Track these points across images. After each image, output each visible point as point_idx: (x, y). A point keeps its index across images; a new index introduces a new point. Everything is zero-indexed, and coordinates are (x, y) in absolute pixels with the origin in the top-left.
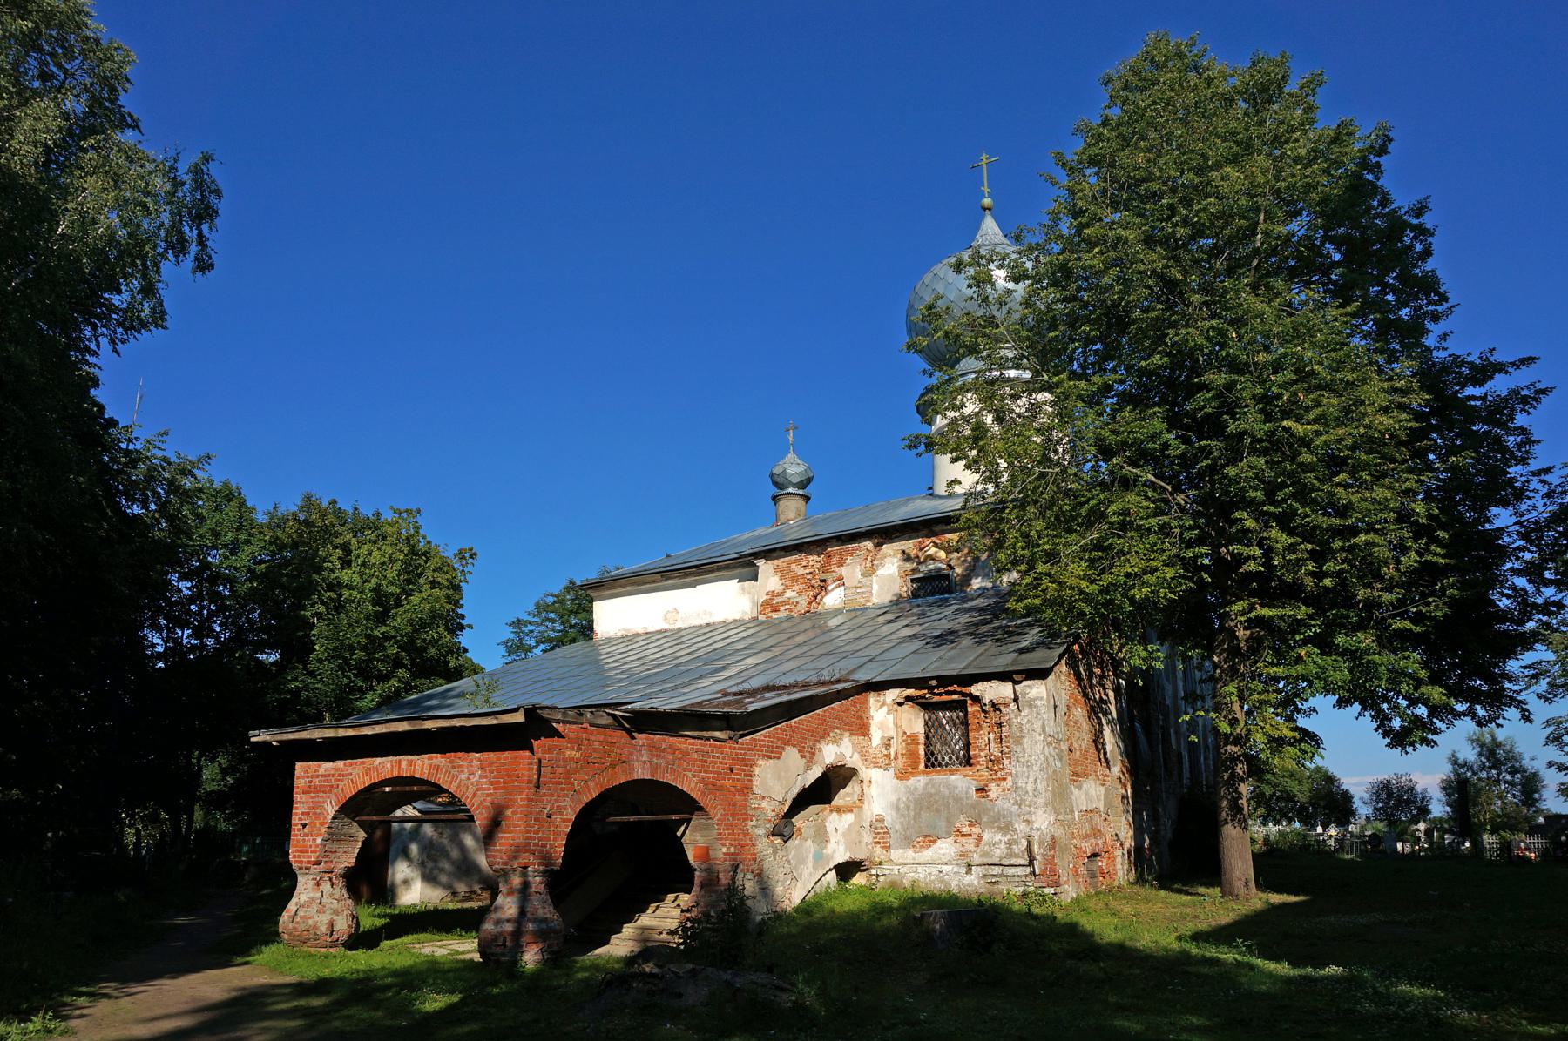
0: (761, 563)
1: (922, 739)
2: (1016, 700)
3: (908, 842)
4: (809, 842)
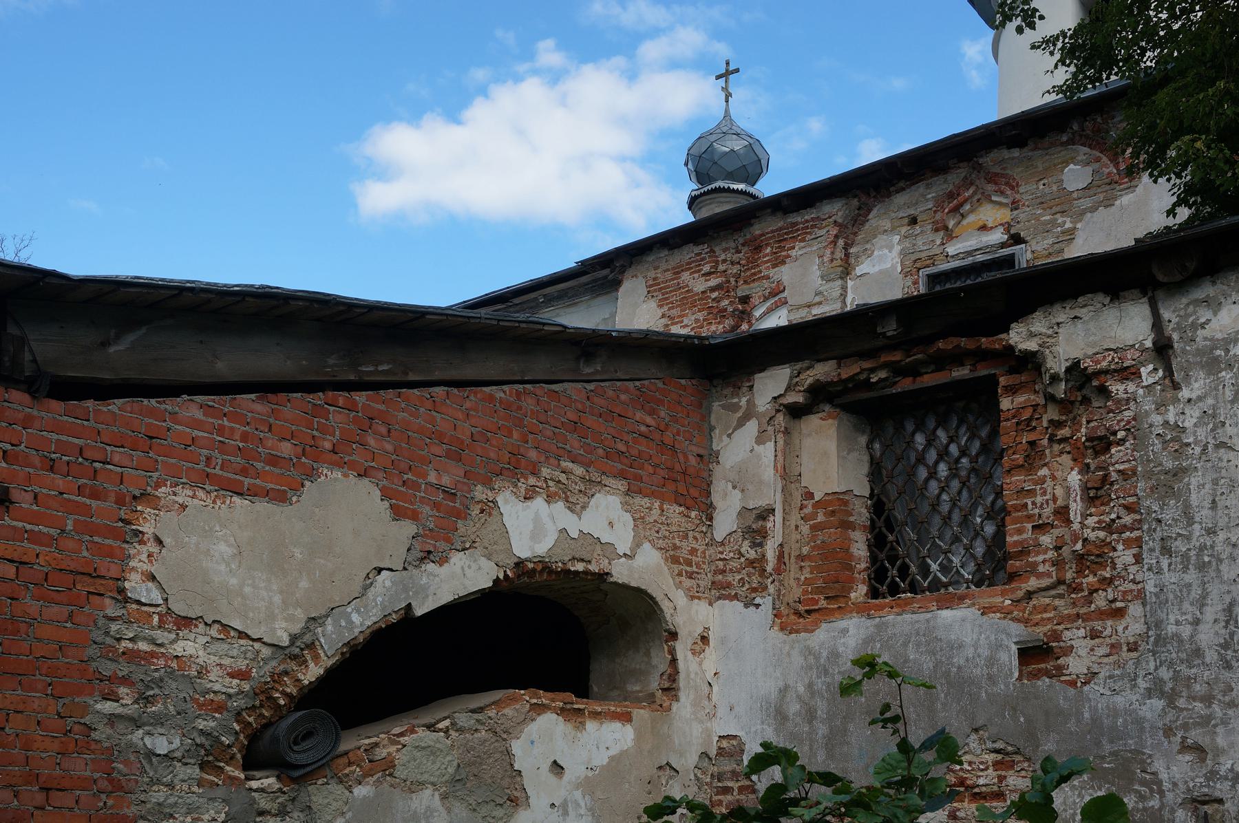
1: (861, 513)
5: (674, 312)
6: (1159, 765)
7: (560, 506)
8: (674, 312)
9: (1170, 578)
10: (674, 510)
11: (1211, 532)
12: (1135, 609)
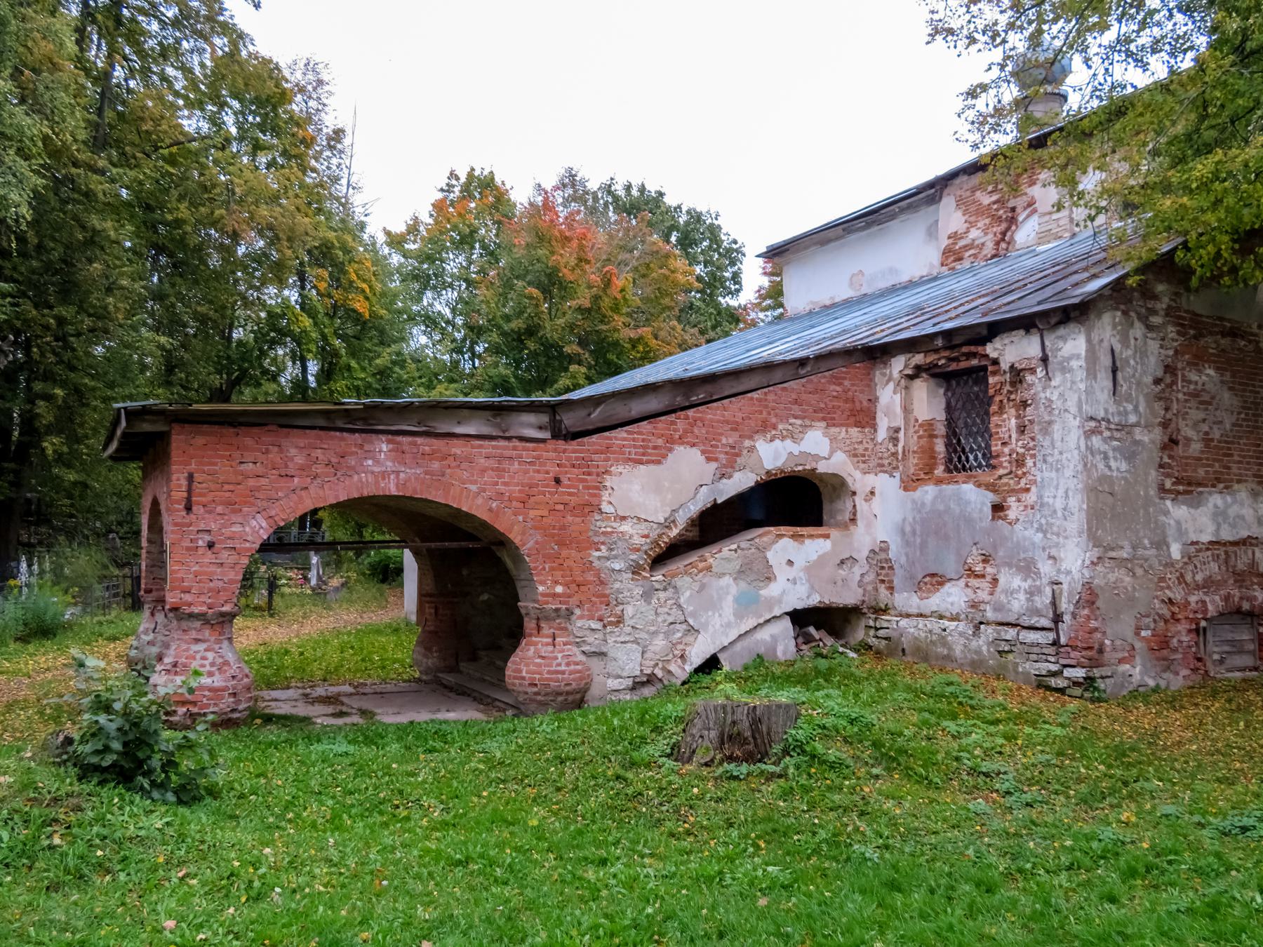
1: (941, 429)
4: (727, 580)
7: (788, 442)
10: (854, 431)
11: (1061, 453)
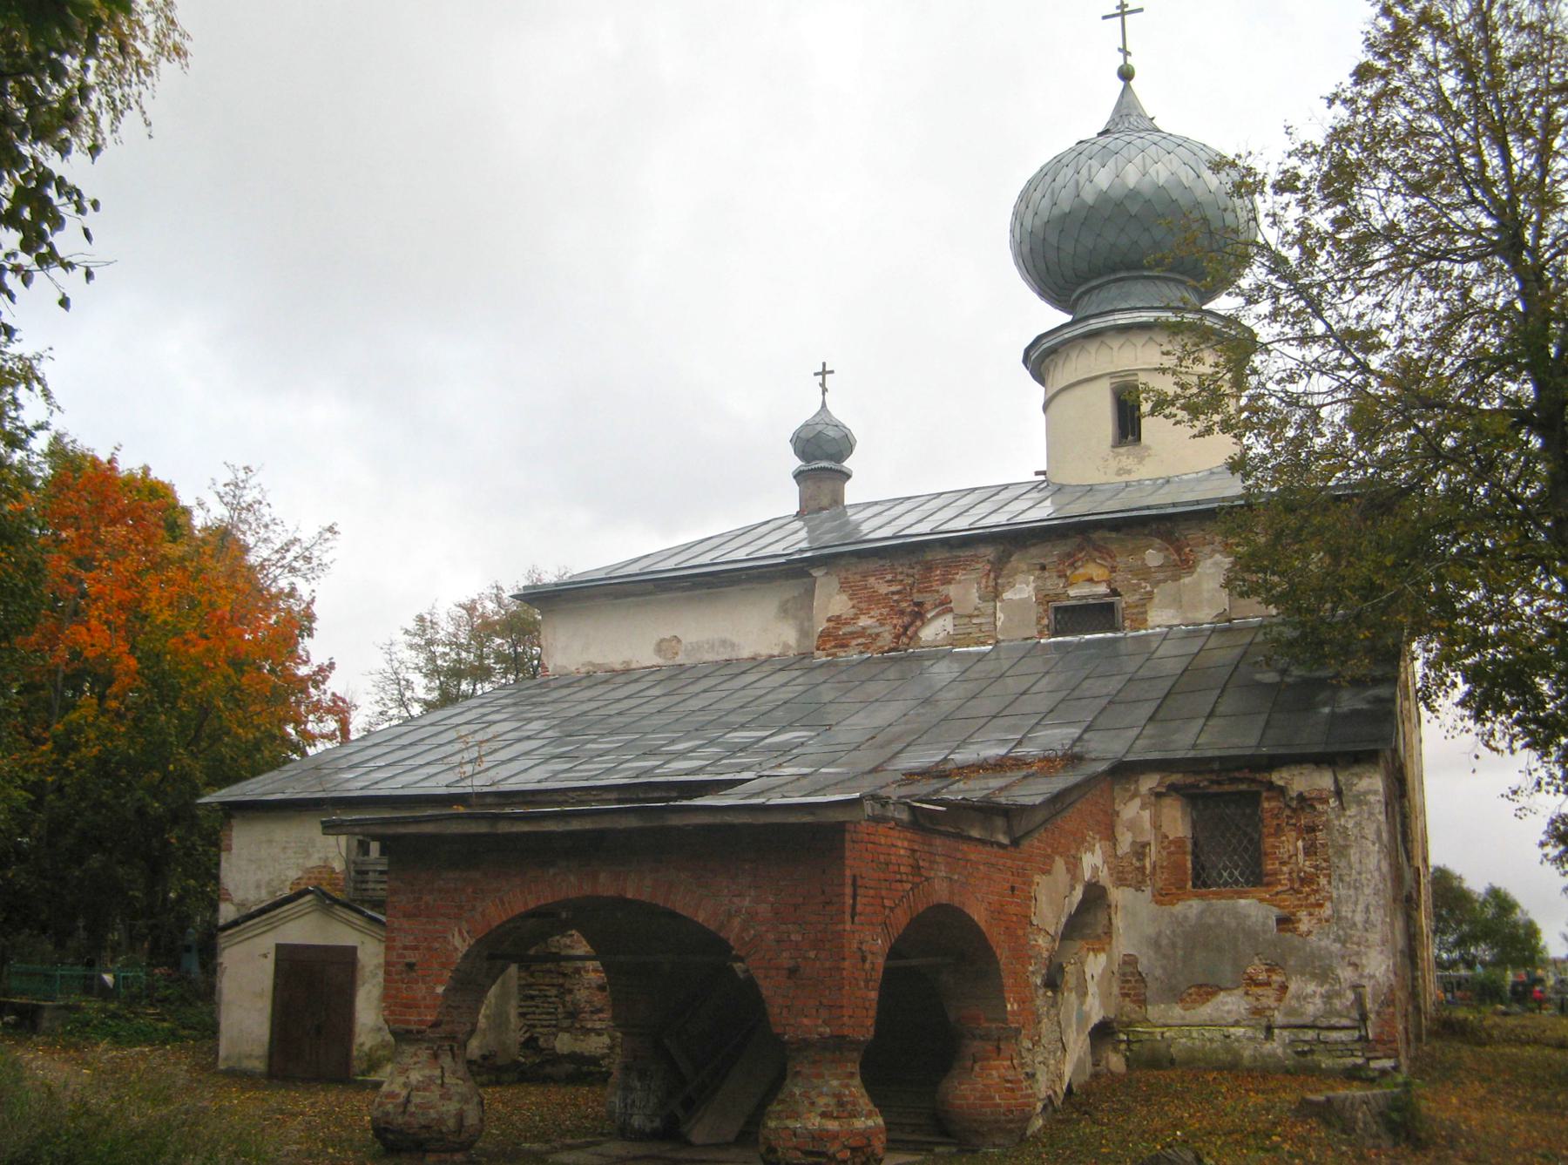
0: (817, 573)
1: (1189, 847)
2: (1339, 793)
3: (1175, 994)
5: (863, 605)
6: (1339, 971)
8: (863, 605)
9: (1343, 892)
12: (1328, 904)
